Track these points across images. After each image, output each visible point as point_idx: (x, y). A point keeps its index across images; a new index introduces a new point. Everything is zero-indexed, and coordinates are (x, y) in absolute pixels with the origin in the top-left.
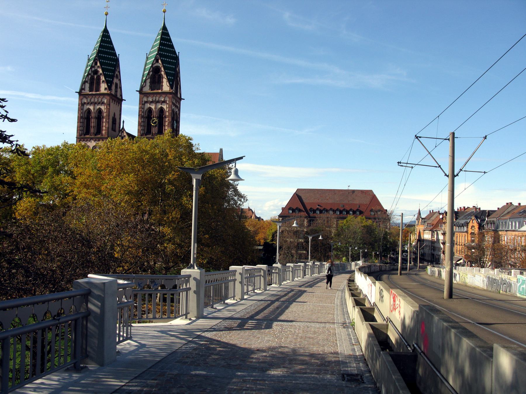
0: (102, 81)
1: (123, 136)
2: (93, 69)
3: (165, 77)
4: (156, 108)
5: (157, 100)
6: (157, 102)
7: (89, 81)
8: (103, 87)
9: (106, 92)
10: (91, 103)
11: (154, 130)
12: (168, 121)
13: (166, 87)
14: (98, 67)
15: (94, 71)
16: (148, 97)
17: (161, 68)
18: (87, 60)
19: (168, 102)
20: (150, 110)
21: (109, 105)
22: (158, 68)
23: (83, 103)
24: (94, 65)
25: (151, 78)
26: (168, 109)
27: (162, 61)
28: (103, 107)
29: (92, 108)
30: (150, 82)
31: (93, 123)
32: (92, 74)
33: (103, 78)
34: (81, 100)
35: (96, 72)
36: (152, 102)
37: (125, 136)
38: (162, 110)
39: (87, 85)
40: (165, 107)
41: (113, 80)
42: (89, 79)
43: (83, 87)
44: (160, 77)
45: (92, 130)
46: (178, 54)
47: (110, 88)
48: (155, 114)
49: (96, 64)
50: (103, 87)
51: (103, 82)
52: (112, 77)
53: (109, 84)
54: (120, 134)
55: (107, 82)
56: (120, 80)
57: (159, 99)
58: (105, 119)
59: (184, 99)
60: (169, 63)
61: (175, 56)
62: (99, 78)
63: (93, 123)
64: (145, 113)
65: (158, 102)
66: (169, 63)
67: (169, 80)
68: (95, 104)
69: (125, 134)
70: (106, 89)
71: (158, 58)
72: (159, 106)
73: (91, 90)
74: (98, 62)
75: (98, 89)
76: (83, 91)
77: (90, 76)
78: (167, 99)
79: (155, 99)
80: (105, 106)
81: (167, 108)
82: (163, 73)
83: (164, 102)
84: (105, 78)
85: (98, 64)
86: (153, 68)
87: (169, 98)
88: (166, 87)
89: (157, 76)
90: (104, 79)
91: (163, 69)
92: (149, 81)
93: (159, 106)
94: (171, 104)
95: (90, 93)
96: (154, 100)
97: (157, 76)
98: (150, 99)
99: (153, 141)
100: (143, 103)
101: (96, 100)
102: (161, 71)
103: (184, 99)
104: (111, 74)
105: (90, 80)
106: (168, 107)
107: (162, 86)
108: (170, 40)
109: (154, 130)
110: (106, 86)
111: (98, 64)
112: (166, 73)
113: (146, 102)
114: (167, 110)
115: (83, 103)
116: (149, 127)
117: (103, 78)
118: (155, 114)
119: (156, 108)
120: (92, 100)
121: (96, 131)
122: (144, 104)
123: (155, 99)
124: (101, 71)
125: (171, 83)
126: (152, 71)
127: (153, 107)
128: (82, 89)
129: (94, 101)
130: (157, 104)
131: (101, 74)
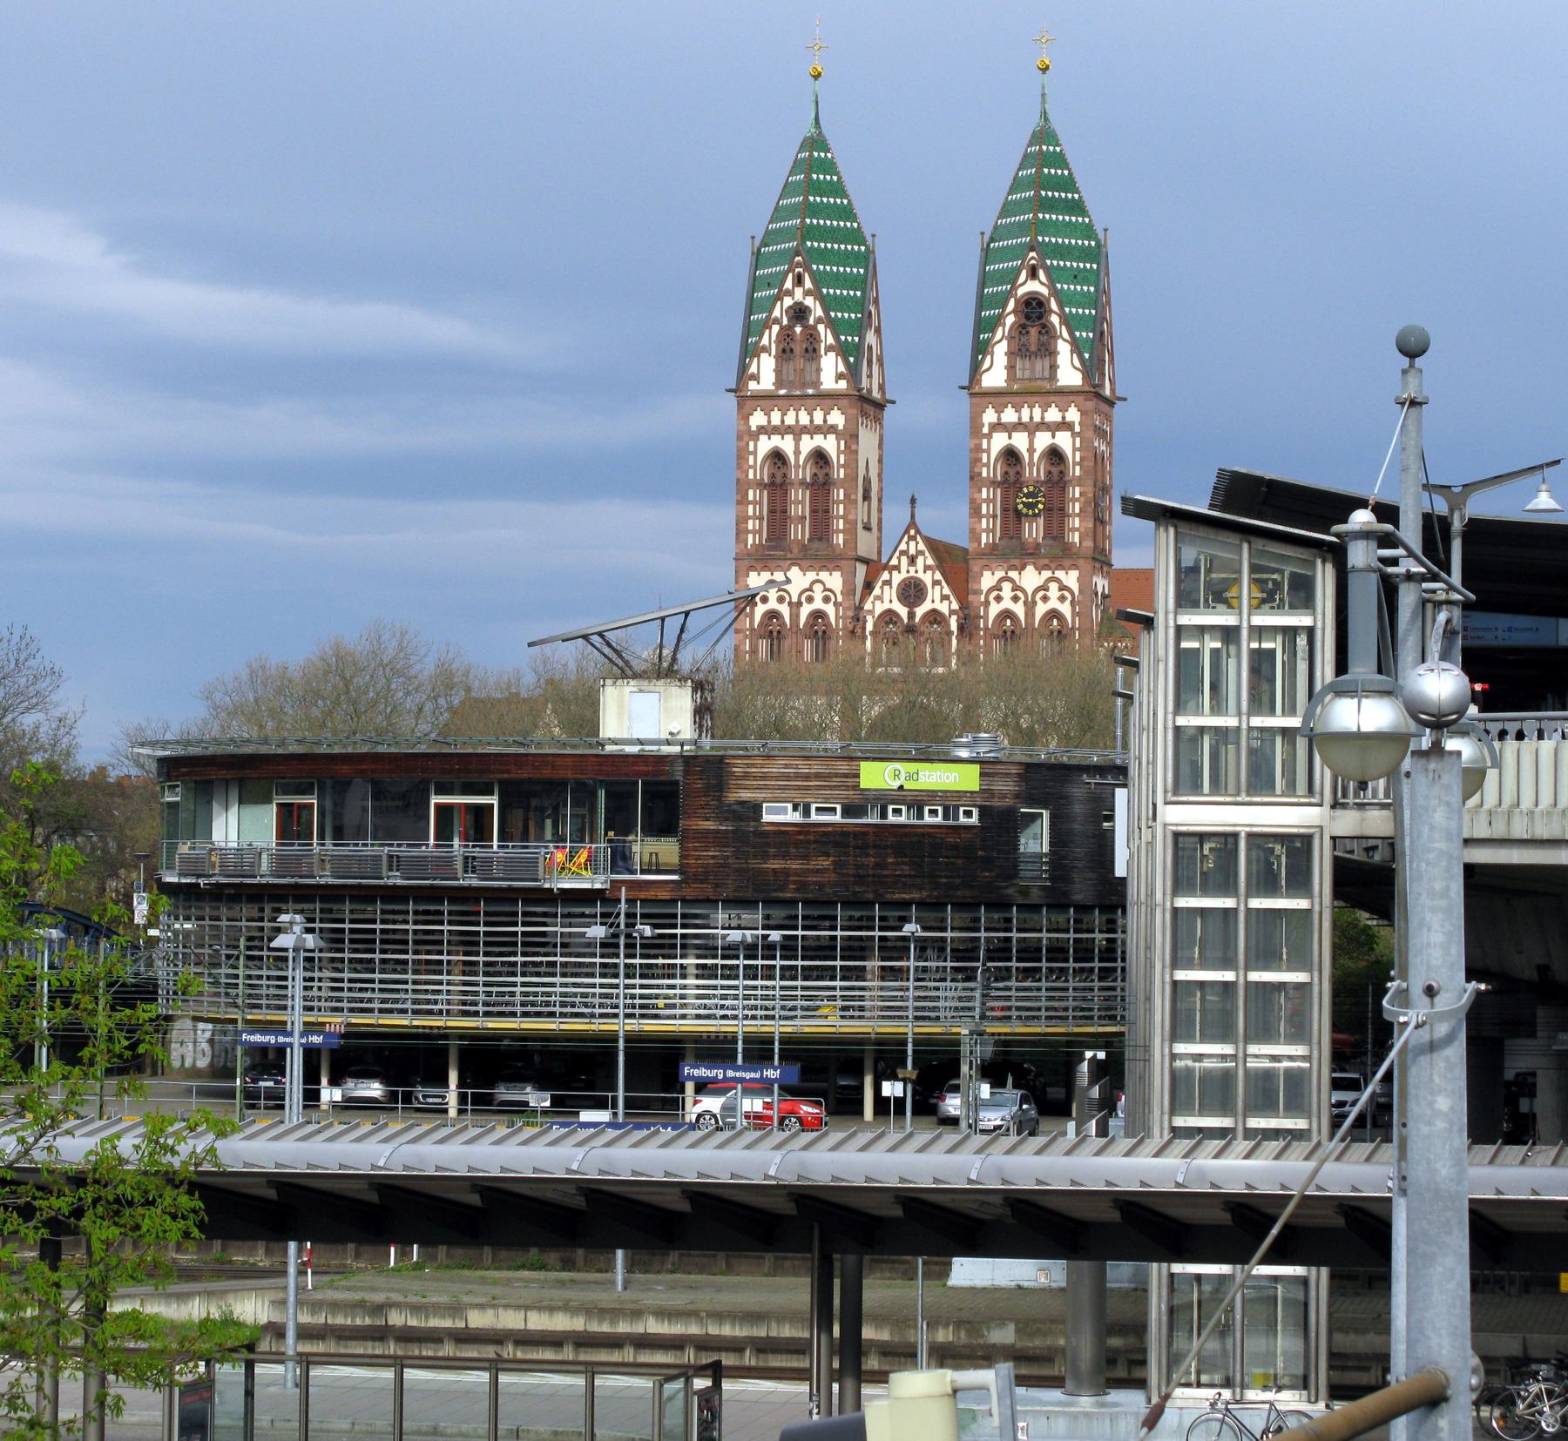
0: (823, 345)
1: (912, 551)
2: (788, 302)
3: (1065, 335)
4: (1031, 450)
5: (1037, 419)
6: (1032, 428)
7: (773, 346)
8: (830, 371)
9: (843, 385)
10: (782, 430)
12: (1083, 499)
14: (807, 293)
15: (790, 307)
16: (999, 411)
17: (1048, 301)
18: (746, 259)
19: (1077, 429)
21: (855, 436)
22: (1035, 299)
23: (754, 428)
24: (788, 284)
25: (1011, 338)
26: (1078, 454)
27: (1048, 270)
28: (830, 445)
29: (786, 444)
30: (1010, 354)
31: (799, 503)
32: (785, 322)
33: (826, 336)
36: (1019, 426)
37: (921, 553)
38: (1054, 454)
40: (1064, 441)
41: (862, 338)
42: (774, 338)
43: (753, 369)
44: (1046, 329)
45: (799, 532)
46: (1101, 236)
47: (852, 374)
48: (1034, 470)
49: (799, 281)
50: (830, 371)
51: (829, 349)
52: (860, 328)
53: (852, 359)
54: (903, 547)
55: (842, 350)
56: (878, 331)
57: (1043, 418)
58: (842, 491)
59: (1125, 399)
60: (1075, 277)
61: (1093, 243)
62: (812, 337)
63: (799, 503)
64: (995, 469)
65: (1044, 426)
66: (1076, 277)
67: (1076, 346)
68: (797, 432)
69: (922, 546)
70: (839, 377)
71: (1033, 262)
74: (806, 275)
76: (752, 385)
77: (776, 328)
78: (1073, 415)
79: (1031, 418)
80: (842, 443)
81: (1075, 449)
82: (1055, 319)
83: (1065, 425)
84: (836, 336)
85: (808, 284)
86: (1017, 302)
87: (1083, 413)
88: (1069, 374)
89: (1033, 331)
90: (830, 340)
91: (1054, 305)
92: (1000, 350)
93: (1043, 440)
94: (1090, 434)
95: (782, 392)
96: (1025, 419)
97: (1033, 331)
98: (1009, 416)
99: (1425, 896)
100: (985, 430)
101: (804, 419)
102: (1051, 311)
103: (1125, 399)
104: (853, 316)
105: (778, 342)
106: (1078, 445)
107: (1054, 367)
110: (842, 368)
111: (808, 284)
112: (1065, 320)
113: (998, 426)
114: (1078, 459)
115: (754, 428)
117: (826, 336)
118: (1034, 470)
119: (1035, 450)
120: (790, 419)
121: (807, 536)
122: (989, 436)
123: (1031, 418)
124: (819, 312)
125: (1087, 355)
126: (1014, 311)
127: (1020, 441)
129: (797, 421)
130: (1038, 434)
131: (819, 320)
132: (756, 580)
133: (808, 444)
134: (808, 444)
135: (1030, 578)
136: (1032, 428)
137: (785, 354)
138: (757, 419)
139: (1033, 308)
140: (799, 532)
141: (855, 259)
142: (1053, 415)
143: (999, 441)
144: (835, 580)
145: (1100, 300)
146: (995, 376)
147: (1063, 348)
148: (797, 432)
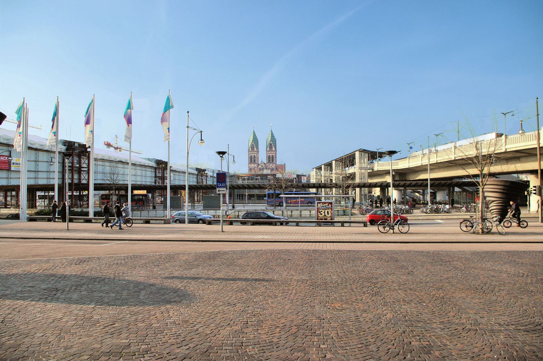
8: (255, 149)
11: (271, 161)
13: (274, 149)
20: (269, 156)
28: (255, 155)
29: (252, 155)
31: (253, 159)
34: (249, 153)
35: (253, 145)
38: (273, 156)
39: (250, 148)
40: (273, 154)
44: (272, 146)
45: (253, 161)
47: (257, 149)
48: (271, 157)
55: (256, 147)
62: (254, 147)
66: (274, 142)
68: (253, 154)
72: (272, 154)
73: (251, 150)
75: (254, 149)
88: (274, 149)
93: (272, 154)
108: (273, 135)
109: (271, 161)
116: (269, 161)
118: (271, 157)
127: (270, 154)
128: (249, 150)
132: (250, 165)
133: (254, 155)
134: (254, 155)
135: (271, 165)
136: (271, 153)
137: (252, 148)
138: (250, 153)
139: (271, 144)
140: (253, 161)
141: (257, 142)
142: (273, 152)
143: (268, 154)
144: (256, 165)
145: (276, 145)
146: (268, 150)
147: (273, 147)
148: (253, 154)
